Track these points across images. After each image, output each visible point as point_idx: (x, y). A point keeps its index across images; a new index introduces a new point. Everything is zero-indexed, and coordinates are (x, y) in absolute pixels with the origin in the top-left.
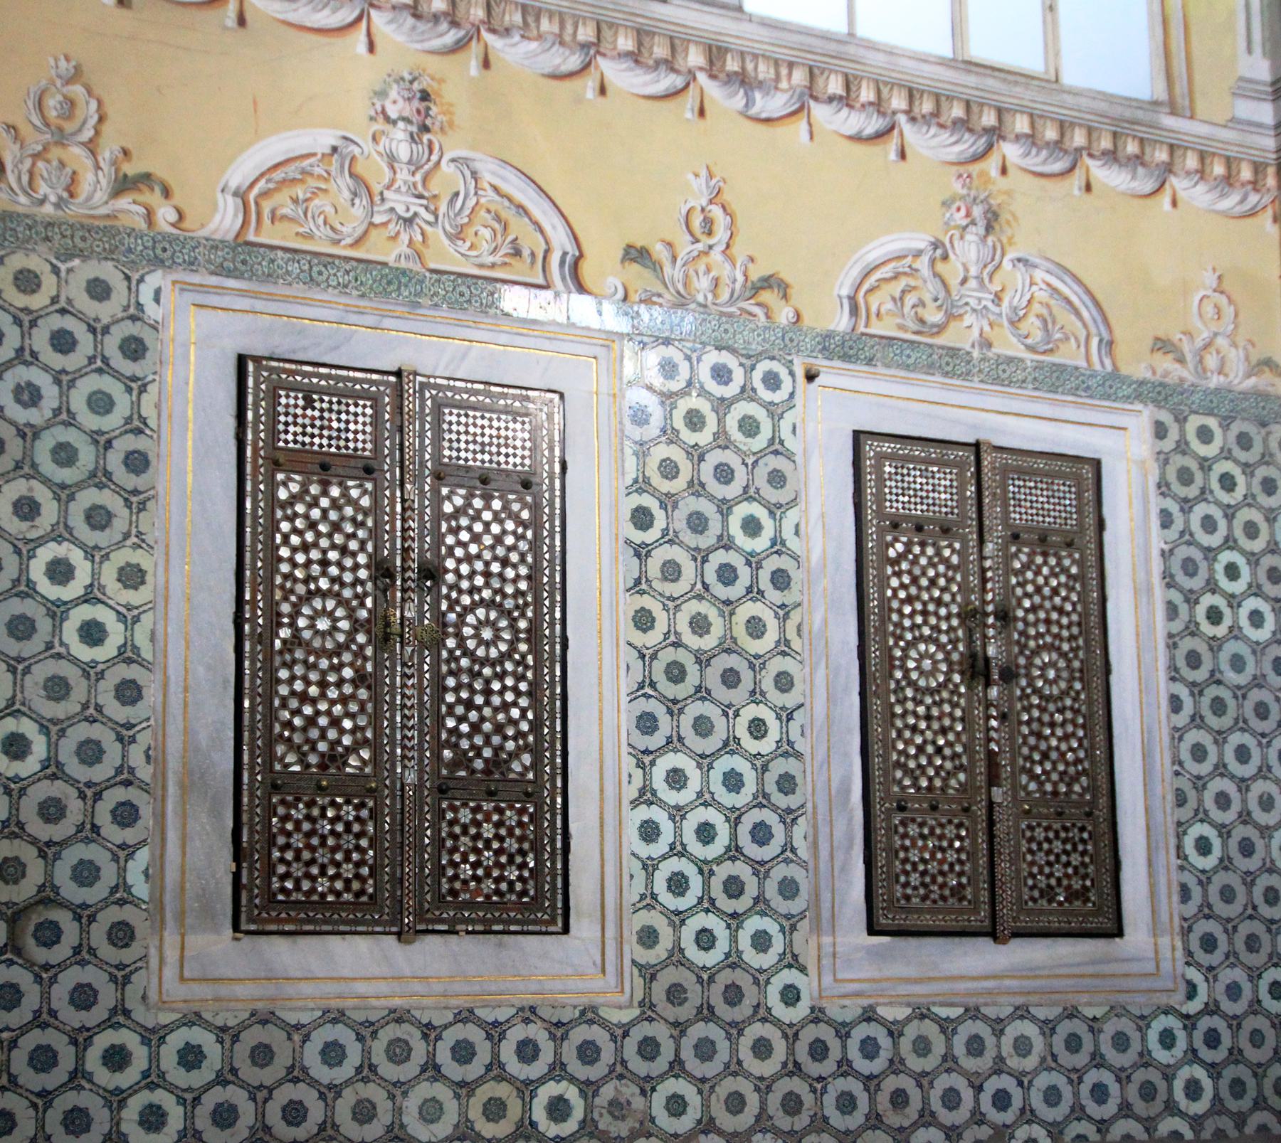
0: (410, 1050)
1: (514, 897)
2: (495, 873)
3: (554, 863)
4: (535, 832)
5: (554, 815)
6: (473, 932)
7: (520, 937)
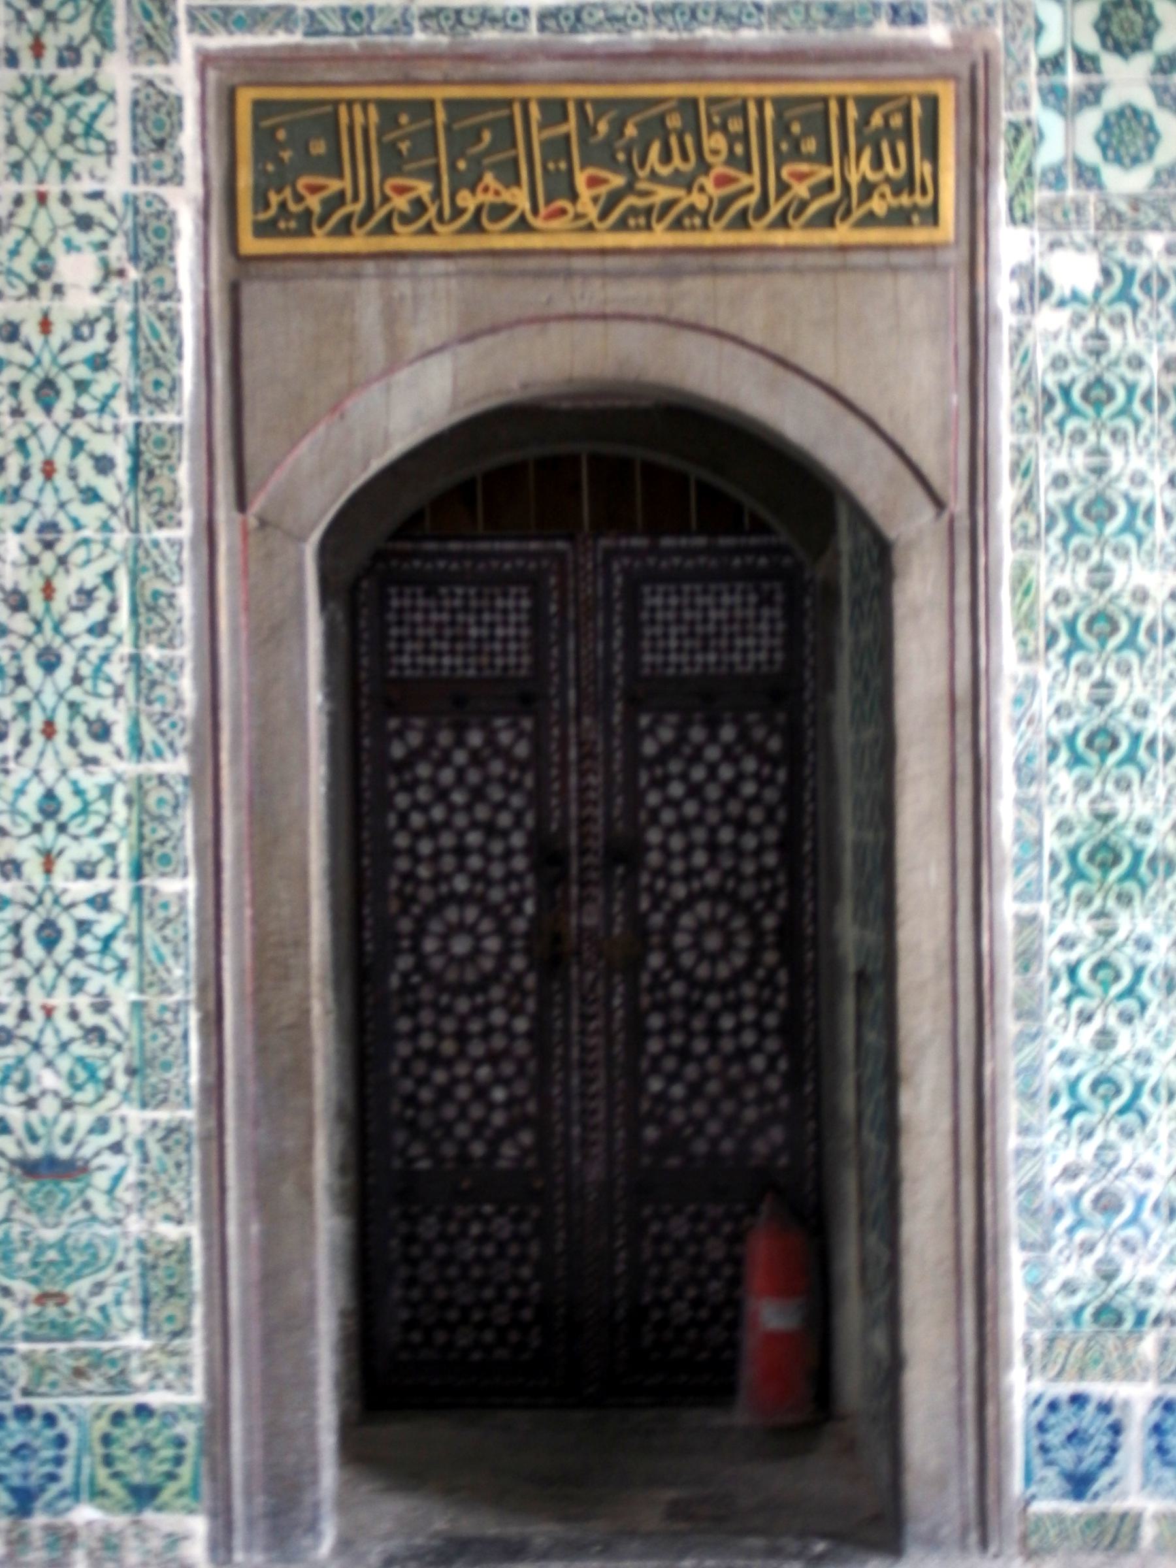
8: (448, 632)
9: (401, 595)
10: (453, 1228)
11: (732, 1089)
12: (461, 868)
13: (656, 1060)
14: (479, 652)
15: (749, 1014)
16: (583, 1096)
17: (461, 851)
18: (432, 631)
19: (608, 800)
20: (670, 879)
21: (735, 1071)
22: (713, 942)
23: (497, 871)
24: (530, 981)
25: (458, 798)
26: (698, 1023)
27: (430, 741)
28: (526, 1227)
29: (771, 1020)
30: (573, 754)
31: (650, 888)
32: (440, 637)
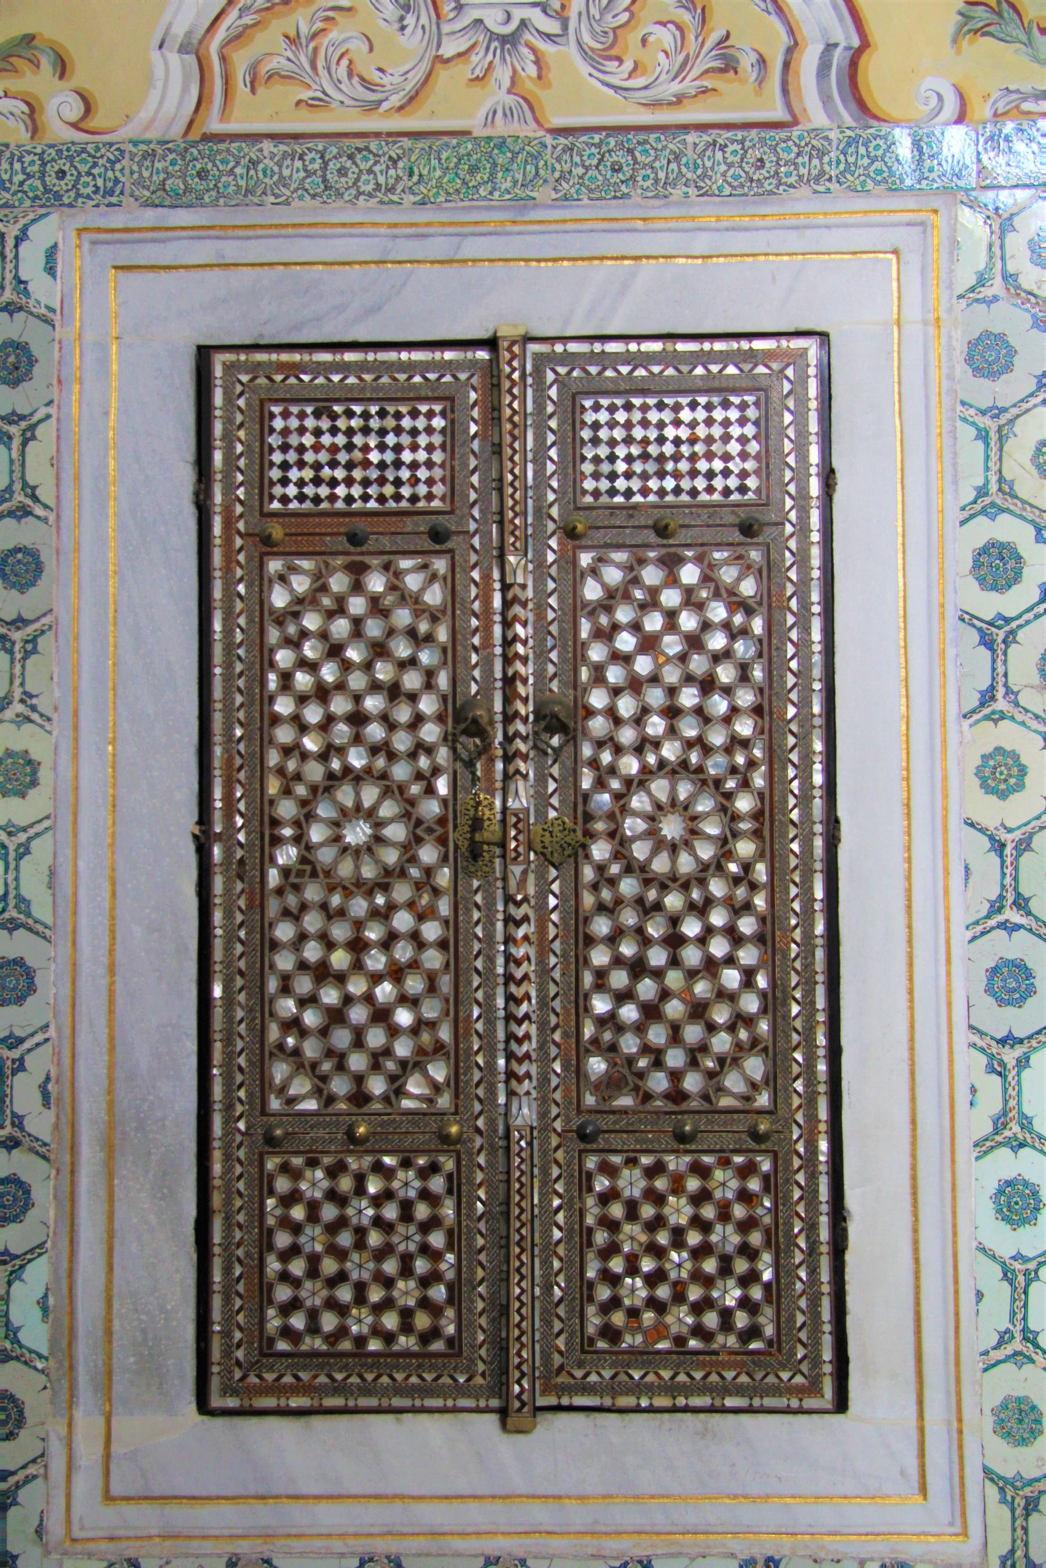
1: (732, 1341)
2: (694, 1293)
3: (813, 1271)
4: (775, 1210)
5: (813, 1177)
6: (651, 1410)
7: (744, 1418)
8: (343, 457)
9: (286, 415)
10: (346, 1184)
11: (698, 1011)
12: (357, 739)
13: (601, 974)
14: (382, 481)
16: (509, 1017)
17: (358, 719)
18: (323, 457)
19: (541, 656)
20: (618, 750)
21: (701, 988)
22: (671, 828)
23: (402, 742)
24: (444, 877)
26: (655, 929)
28: (437, 1184)
29: (747, 925)
31: (594, 763)
32: (333, 464)
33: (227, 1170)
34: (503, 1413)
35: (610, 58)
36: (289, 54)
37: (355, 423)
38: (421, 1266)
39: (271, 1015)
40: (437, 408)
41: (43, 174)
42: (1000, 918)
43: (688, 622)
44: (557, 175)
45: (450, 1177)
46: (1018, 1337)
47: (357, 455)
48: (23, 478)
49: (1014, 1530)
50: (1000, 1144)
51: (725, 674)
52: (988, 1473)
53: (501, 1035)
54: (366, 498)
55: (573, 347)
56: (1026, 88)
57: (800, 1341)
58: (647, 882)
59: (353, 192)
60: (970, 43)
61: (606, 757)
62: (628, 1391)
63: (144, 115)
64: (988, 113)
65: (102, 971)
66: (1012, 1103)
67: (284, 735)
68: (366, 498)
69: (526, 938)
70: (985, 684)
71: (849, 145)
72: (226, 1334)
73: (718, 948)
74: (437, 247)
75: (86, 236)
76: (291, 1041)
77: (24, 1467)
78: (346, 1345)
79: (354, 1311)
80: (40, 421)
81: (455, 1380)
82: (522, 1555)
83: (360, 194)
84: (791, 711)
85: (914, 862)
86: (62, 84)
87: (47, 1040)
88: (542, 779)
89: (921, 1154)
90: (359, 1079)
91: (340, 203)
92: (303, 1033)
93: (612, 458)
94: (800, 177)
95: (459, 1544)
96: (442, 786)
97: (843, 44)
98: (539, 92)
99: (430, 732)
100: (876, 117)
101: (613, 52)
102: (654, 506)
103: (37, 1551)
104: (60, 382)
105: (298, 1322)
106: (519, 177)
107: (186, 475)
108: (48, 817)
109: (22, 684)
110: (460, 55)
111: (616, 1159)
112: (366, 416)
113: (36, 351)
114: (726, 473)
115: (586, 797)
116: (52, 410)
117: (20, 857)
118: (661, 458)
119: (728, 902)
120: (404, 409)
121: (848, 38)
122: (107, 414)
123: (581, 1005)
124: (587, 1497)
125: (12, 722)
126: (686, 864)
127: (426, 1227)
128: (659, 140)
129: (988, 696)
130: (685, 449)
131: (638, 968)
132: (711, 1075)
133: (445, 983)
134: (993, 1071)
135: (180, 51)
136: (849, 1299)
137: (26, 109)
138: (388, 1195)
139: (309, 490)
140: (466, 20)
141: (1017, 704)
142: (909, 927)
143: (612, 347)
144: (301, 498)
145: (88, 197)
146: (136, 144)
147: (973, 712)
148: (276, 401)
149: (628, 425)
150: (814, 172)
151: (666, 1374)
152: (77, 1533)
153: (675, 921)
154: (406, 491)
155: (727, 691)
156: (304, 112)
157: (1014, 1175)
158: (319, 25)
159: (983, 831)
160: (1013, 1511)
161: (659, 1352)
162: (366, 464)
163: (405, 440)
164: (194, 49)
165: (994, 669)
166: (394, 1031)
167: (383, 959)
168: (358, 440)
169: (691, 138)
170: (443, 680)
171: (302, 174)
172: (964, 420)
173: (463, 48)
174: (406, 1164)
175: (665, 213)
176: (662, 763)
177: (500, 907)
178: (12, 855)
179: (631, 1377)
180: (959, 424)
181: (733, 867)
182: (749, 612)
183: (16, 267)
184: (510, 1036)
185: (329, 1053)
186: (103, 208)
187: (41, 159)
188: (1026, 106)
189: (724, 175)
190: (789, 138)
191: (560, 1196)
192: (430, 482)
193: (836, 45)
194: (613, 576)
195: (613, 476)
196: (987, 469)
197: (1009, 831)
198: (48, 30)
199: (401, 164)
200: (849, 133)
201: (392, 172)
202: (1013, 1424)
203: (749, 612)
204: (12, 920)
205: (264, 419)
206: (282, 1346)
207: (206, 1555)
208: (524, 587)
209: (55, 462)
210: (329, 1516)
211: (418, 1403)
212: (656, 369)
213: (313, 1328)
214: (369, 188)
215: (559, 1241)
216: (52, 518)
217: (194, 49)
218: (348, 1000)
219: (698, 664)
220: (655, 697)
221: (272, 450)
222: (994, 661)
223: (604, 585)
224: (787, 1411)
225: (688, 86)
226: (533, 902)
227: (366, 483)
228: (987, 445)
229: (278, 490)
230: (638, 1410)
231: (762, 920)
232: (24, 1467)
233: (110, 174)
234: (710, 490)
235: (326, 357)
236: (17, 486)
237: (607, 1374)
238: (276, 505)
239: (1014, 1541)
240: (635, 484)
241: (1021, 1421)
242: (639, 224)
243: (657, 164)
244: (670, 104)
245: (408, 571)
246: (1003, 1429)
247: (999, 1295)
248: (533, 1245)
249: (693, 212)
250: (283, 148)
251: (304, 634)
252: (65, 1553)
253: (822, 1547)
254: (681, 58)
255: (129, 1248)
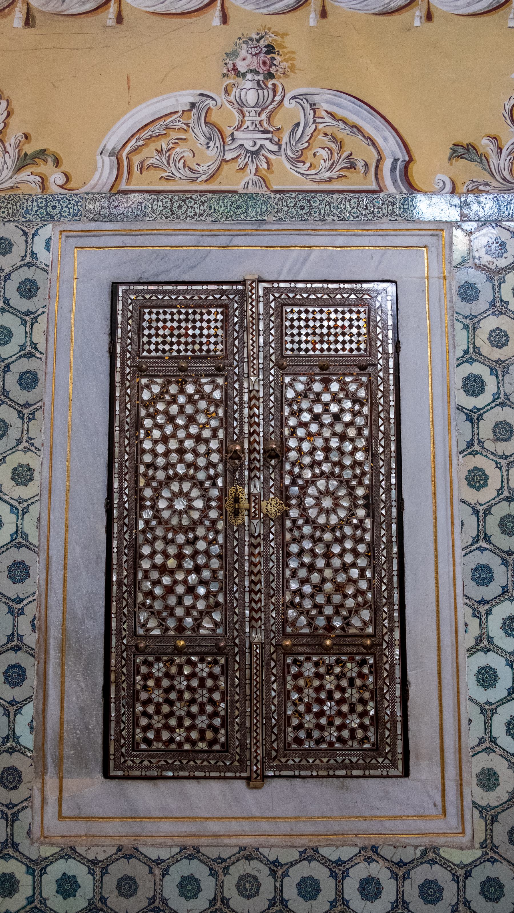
0: (259, 885)
6: (318, 776)
9: (150, 313)
12: (181, 461)
14: (194, 343)
15: (348, 545)
17: (181, 451)
18: (167, 332)
19: (267, 422)
23: (202, 462)
25: (180, 421)
27: (164, 391)
28: (217, 670)
30: (246, 398)
31: (291, 473)
32: (172, 335)
33: (118, 663)
34: (248, 779)
35: (300, 162)
36: (158, 157)
37: (182, 317)
38: (209, 709)
39: (139, 589)
40: (220, 310)
41: (46, 207)
42: (477, 545)
43: (334, 408)
44: (276, 210)
45: (222, 666)
46: (488, 741)
47: (183, 331)
48: (31, 340)
49: (486, 830)
50: (478, 650)
51: (352, 432)
52: (474, 804)
53: (247, 599)
54: (186, 350)
55: (282, 285)
56: (481, 180)
57: (387, 743)
58: (315, 528)
59: (184, 216)
60: (456, 161)
61: (297, 470)
62: (307, 769)
63: (92, 182)
64: (465, 190)
65: (61, 567)
66: (484, 631)
67: (148, 458)
68: (186, 350)
69: (259, 553)
70: (469, 438)
71: (405, 201)
72: (117, 741)
73: (349, 558)
74: (222, 240)
75: (64, 234)
76: (148, 601)
77: (22, 802)
78: (173, 747)
79: (177, 730)
80: (40, 315)
81: (225, 764)
82: (257, 846)
83: (187, 217)
84: (381, 450)
85: (438, 520)
86: (57, 169)
87: (34, 600)
88: (267, 478)
89: (443, 655)
90: (180, 620)
91: (178, 220)
92: (154, 598)
93: (299, 334)
94: (384, 214)
95: (227, 841)
96: (220, 482)
97: (401, 159)
98: (269, 175)
99: (215, 458)
100: (416, 190)
101: (301, 159)
102: (318, 356)
103: (28, 842)
104: (49, 297)
105: (151, 735)
106: (259, 210)
107: (106, 340)
108: (37, 495)
109: (27, 434)
110: (233, 159)
111: (302, 658)
112: (187, 314)
113: (39, 283)
114: (351, 342)
115: (287, 488)
116: (46, 310)
117: (24, 514)
118: (322, 335)
119: (353, 537)
120: (204, 311)
121: (403, 157)
122: (70, 312)
123: (285, 586)
124: (287, 818)
125: (22, 451)
126: (334, 520)
127: (211, 691)
128: (321, 196)
129: (470, 444)
130: (333, 331)
131: (311, 568)
132: (345, 618)
133: (221, 574)
134: (476, 616)
135: (109, 156)
136: (410, 723)
137: (40, 180)
138: (193, 675)
139: (161, 347)
140: (236, 145)
141: (483, 448)
142: (436, 549)
143: (300, 285)
144: (157, 350)
145: (66, 217)
146: (88, 194)
147: (464, 450)
148: (146, 307)
149: (307, 320)
150: (390, 212)
151: (325, 760)
152: (46, 833)
153: (328, 546)
154: (205, 348)
155: (352, 440)
156: (163, 181)
157: (485, 664)
158: (171, 146)
159: (469, 505)
160: (486, 822)
161: (321, 749)
162: (187, 335)
163: (205, 325)
164: (116, 154)
165: (473, 432)
166: (197, 597)
167: (192, 563)
168: (183, 324)
169: (335, 196)
170: (221, 434)
171: (162, 208)
172: (458, 320)
173: (234, 156)
174: (202, 660)
175: (324, 227)
176: (322, 473)
177: (247, 539)
178: (20, 513)
179: (308, 762)
180: (455, 322)
181: (355, 521)
182: (362, 405)
183: (32, 247)
184: (251, 600)
185: (166, 607)
186: (72, 222)
187: (46, 200)
188: (481, 188)
189: (350, 212)
190: (379, 197)
191: (275, 675)
192: (216, 343)
193: (398, 159)
194: (300, 387)
195: (300, 342)
196: (468, 342)
197: (481, 505)
198: (52, 147)
199: (206, 204)
200: (405, 196)
201: (202, 208)
202: (485, 781)
203: (362, 405)
204: (19, 543)
205: (141, 314)
206: (143, 746)
207: (107, 846)
208: (258, 391)
209: (46, 333)
210: (166, 827)
211: (207, 774)
212: (319, 296)
213: (158, 737)
214: (192, 214)
215: (274, 697)
216: (43, 358)
217: (116, 154)
218: (175, 582)
219: (339, 428)
220: (319, 443)
221: (144, 329)
222: (473, 428)
223: (295, 391)
224: (381, 776)
225: (334, 174)
226: (262, 537)
227: (186, 344)
228: (468, 331)
229: (146, 347)
230: (312, 777)
231: (368, 545)
232: (22, 802)
233: (76, 207)
234: (344, 349)
235: (169, 288)
236: (28, 344)
237: (297, 760)
238: (145, 353)
239: (486, 836)
240: (310, 346)
241: (489, 780)
242: (312, 232)
243: (320, 207)
244: (326, 181)
245: (205, 384)
246: (481, 784)
247: (479, 721)
248: (263, 699)
249: (336, 227)
250: (153, 196)
251: (157, 412)
252: (41, 843)
253: (398, 841)
254: (331, 162)
255: (73, 696)
